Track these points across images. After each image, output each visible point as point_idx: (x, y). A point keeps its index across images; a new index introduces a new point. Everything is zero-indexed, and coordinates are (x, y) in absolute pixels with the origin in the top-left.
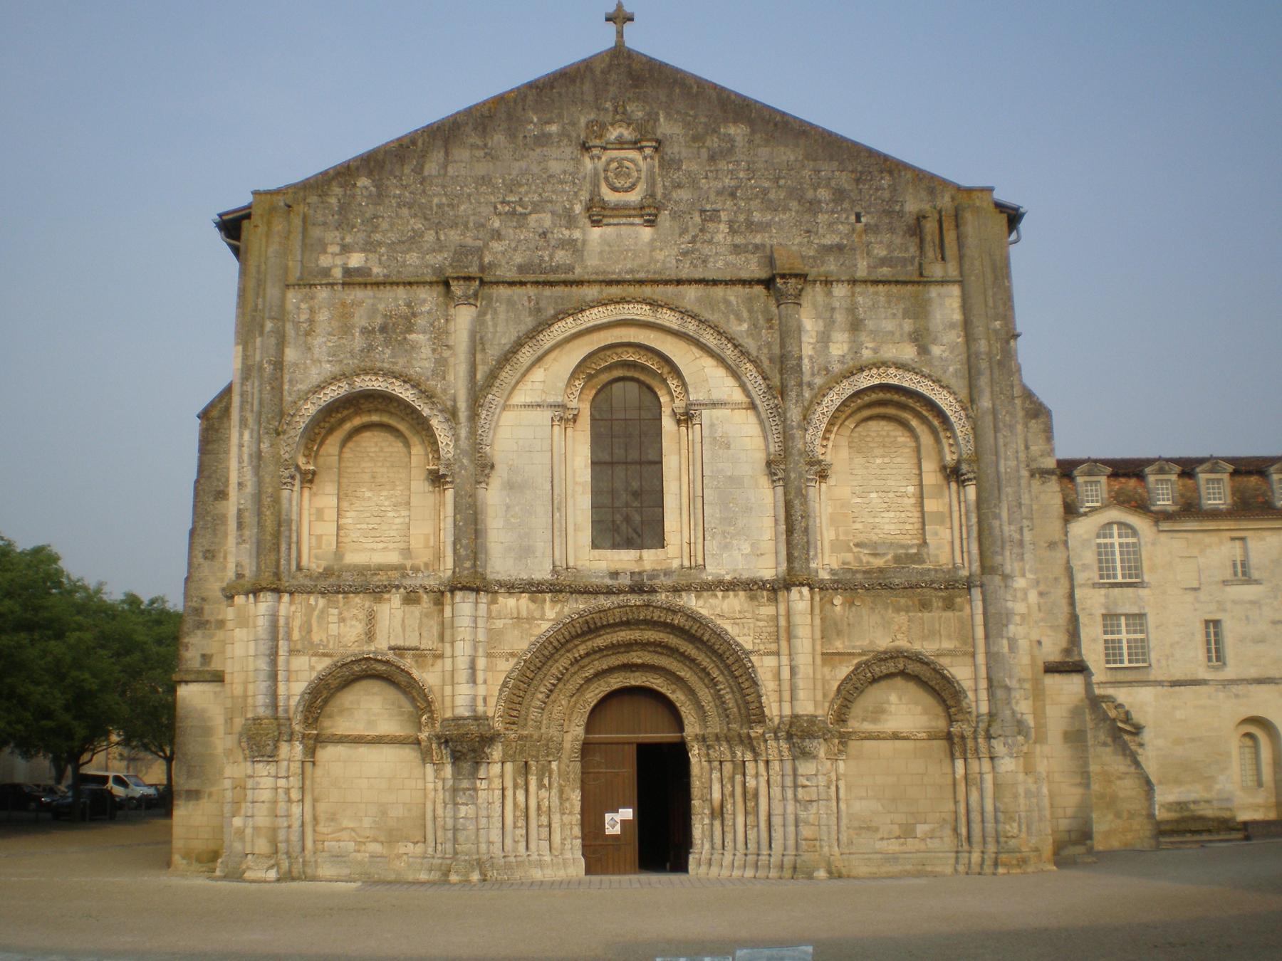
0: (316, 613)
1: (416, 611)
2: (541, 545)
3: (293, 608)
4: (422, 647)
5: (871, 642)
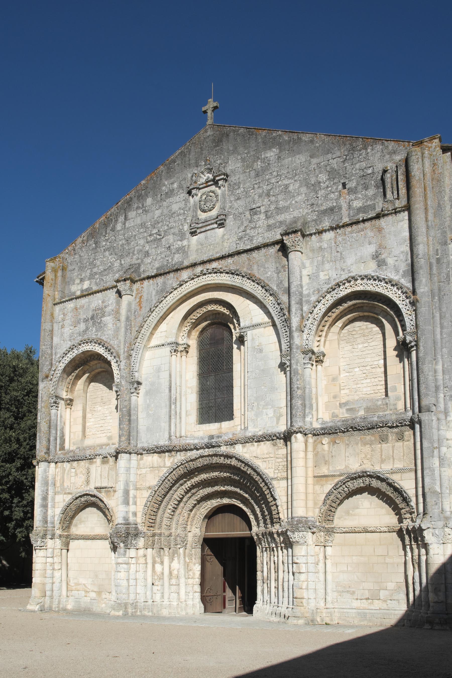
1: (106, 467)
2: (165, 425)
5: (346, 467)
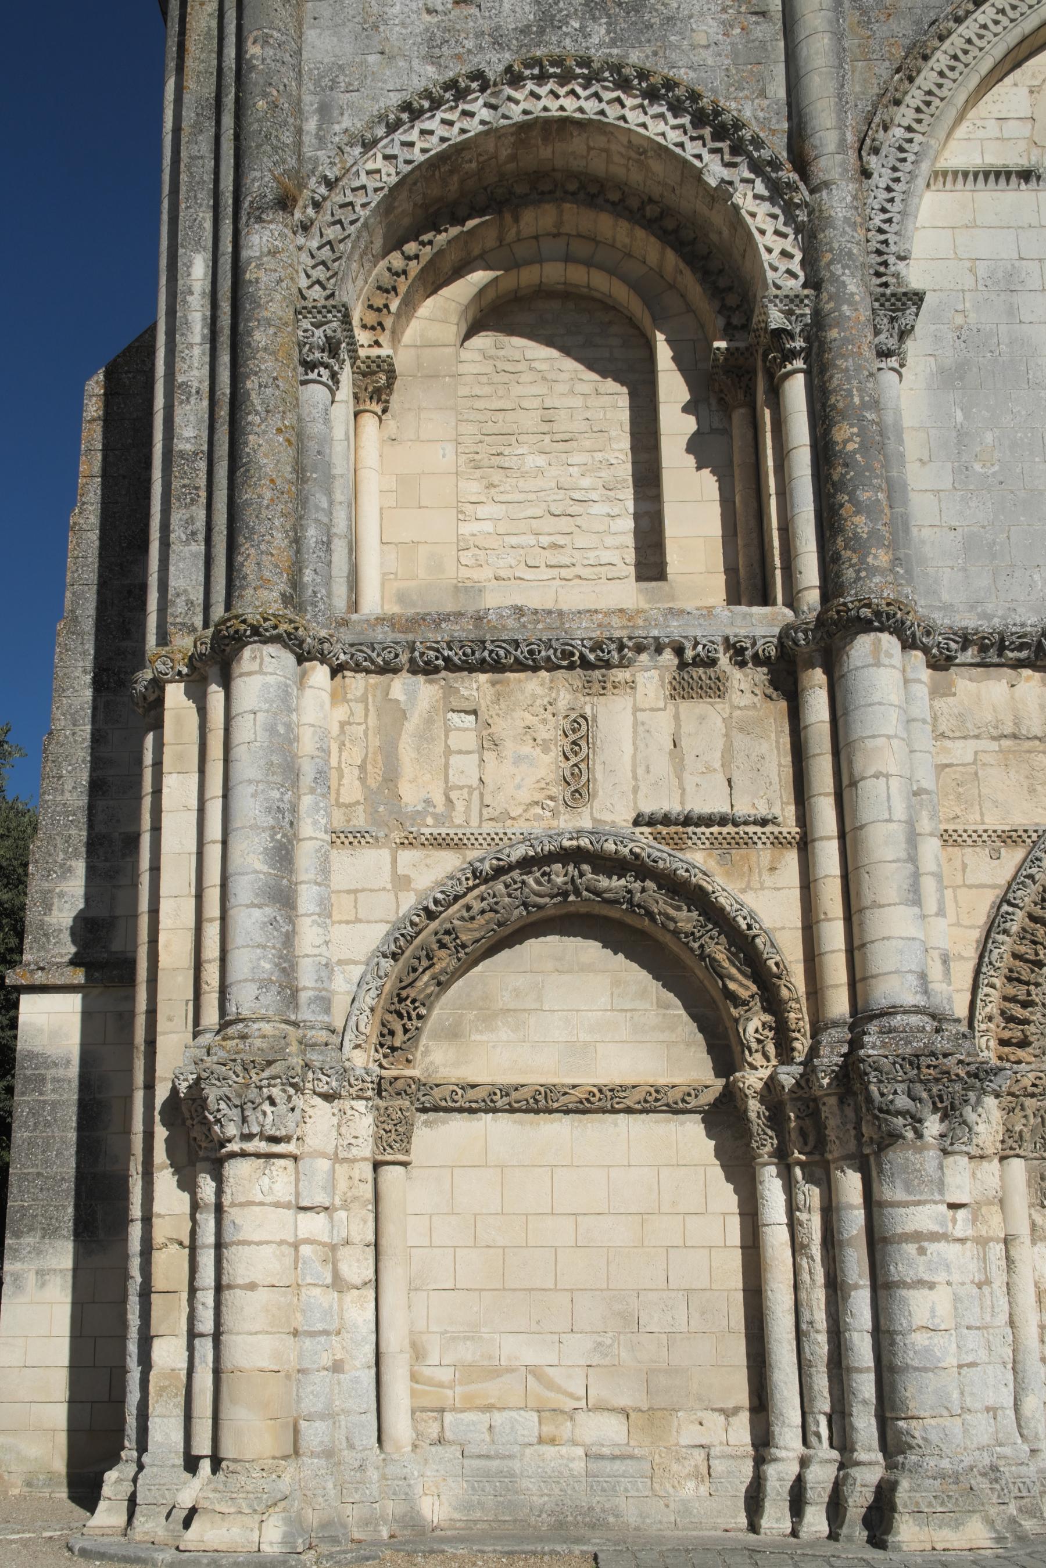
0: (412, 725)
3: (341, 713)
4: (742, 810)
